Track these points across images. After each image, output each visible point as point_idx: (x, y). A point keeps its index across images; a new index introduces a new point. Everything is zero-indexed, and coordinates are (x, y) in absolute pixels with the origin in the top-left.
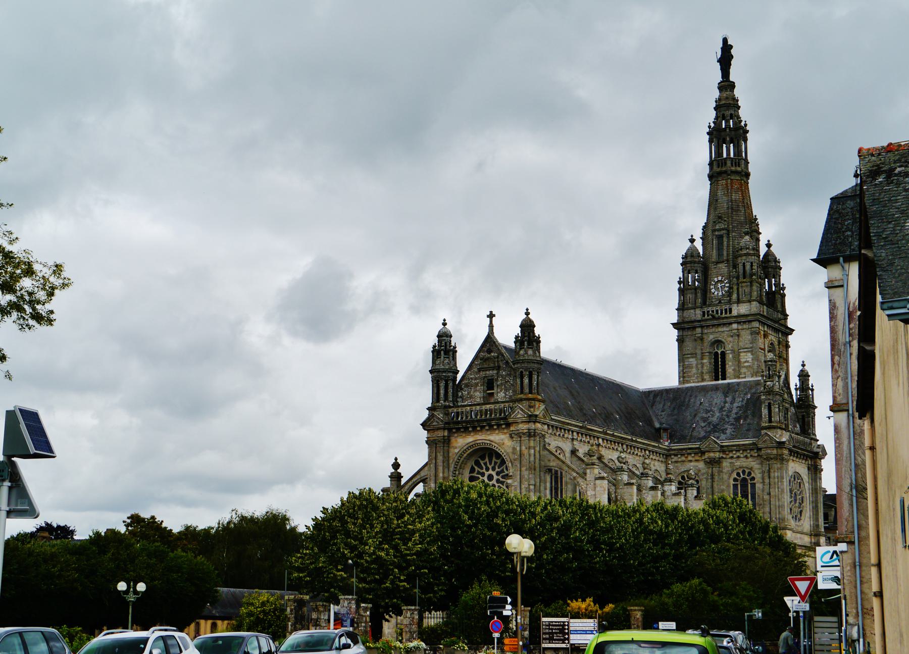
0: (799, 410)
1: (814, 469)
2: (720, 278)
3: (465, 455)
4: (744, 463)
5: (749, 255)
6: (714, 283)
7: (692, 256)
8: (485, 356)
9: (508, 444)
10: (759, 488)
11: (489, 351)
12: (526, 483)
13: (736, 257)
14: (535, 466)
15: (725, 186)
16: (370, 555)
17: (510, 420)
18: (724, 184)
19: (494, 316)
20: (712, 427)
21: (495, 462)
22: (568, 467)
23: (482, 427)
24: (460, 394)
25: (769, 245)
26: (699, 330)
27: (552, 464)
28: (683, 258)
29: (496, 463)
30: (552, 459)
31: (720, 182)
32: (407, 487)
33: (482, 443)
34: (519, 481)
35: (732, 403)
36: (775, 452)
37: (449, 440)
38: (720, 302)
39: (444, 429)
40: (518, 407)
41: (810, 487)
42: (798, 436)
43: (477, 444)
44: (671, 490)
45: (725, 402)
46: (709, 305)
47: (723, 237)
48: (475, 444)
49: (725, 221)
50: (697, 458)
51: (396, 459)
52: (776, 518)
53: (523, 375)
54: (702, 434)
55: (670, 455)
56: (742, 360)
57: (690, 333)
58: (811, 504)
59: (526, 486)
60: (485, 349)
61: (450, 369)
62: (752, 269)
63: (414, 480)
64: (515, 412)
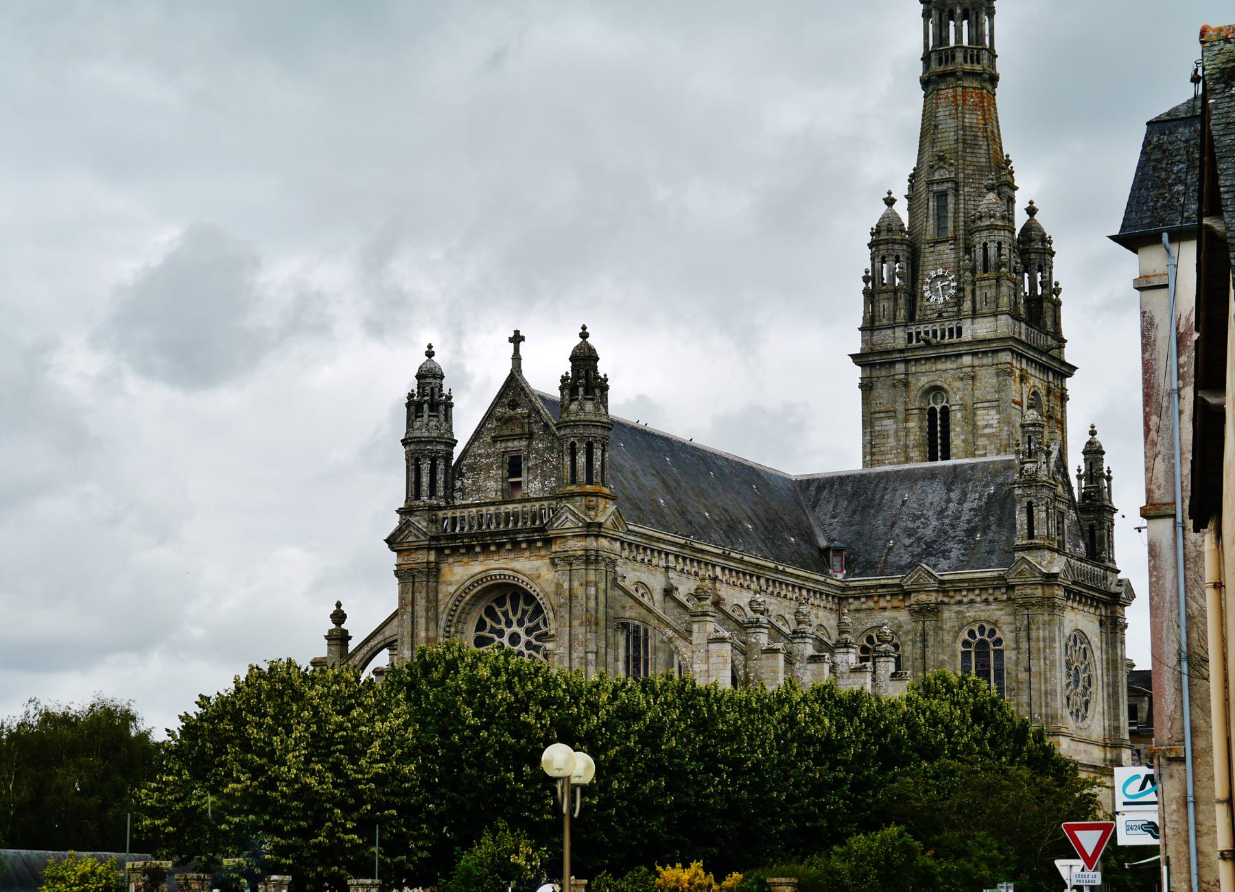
0: (1084, 516)
1: (1111, 624)
2: (940, 272)
3: (468, 597)
4: (982, 614)
5: (995, 229)
7: (889, 230)
8: (506, 413)
9: (546, 577)
10: (1010, 658)
11: (513, 405)
13: (970, 233)
14: (597, 618)
15: (951, 99)
16: (290, 783)
17: (552, 533)
18: (949, 95)
19: (523, 339)
20: (924, 547)
21: (523, 609)
22: (659, 620)
23: (500, 546)
24: (458, 484)
25: (1031, 211)
26: (900, 368)
27: (627, 614)
28: (872, 234)
29: (524, 612)
30: (628, 605)
31: (942, 92)
32: (359, 657)
33: (500, 575)
34: (567, 644)
35: (961, 502)
36: (1039, 592)
37: (438, 570)
38: (940, 316)
39: (429, 549)
40: (565, 508)
41: (1104, 657)
42: (1083, 564)
43: (491, 576)
44: (847, 663)
45: (949, 501)
46: (921, 322)
47: (947, 195)
48: (486, 578)
49: (951, 164)
50: (896, 603)
51: (339, 605)
52: (1040, 715)
53: (575, 449)
54: (906, 559)
55: (847, 598)
56: (979, 423)
57: (883, 373)
58: (1105, 689)
59: (581, 655)
60: (506, 401)
61: (440, 438)
62: (1000, 255)
63: (372, 643)
64: (560, 517)
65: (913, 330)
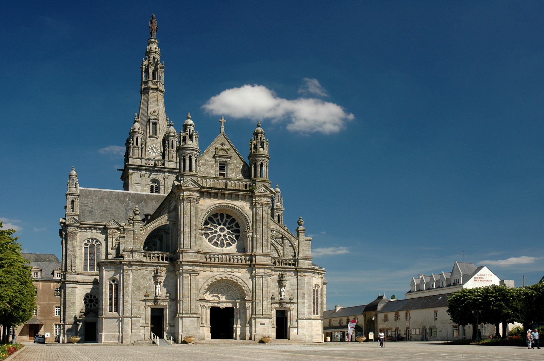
21: (225, 220)
60: (220, 143)
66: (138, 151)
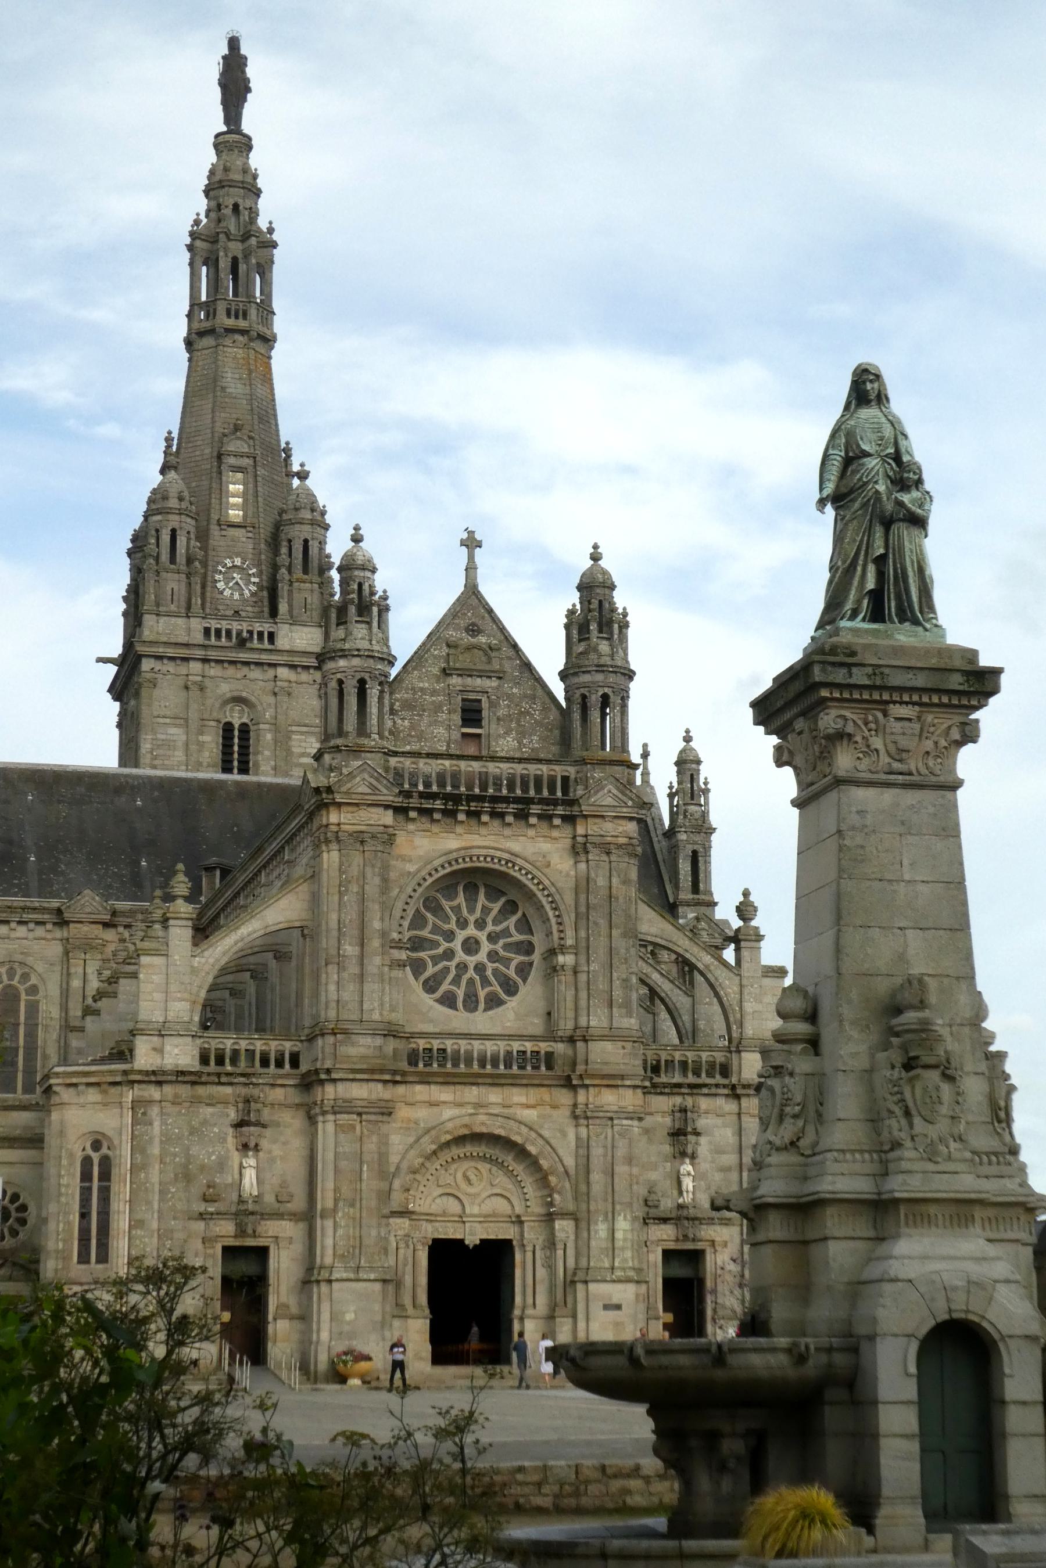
2: (238, 561)
6: (223, 570)
11: (473, 630)
12: (624, 966)
15: (241, 361)
19: (479, 545)
29: (486, 910)
31: (229, 350)
33: (485, 857)
39: (387, 807)
56: (296, 750)
59: (624, 976)
60: (463, 623)
65: (214, 624)
66: (174, 583)
